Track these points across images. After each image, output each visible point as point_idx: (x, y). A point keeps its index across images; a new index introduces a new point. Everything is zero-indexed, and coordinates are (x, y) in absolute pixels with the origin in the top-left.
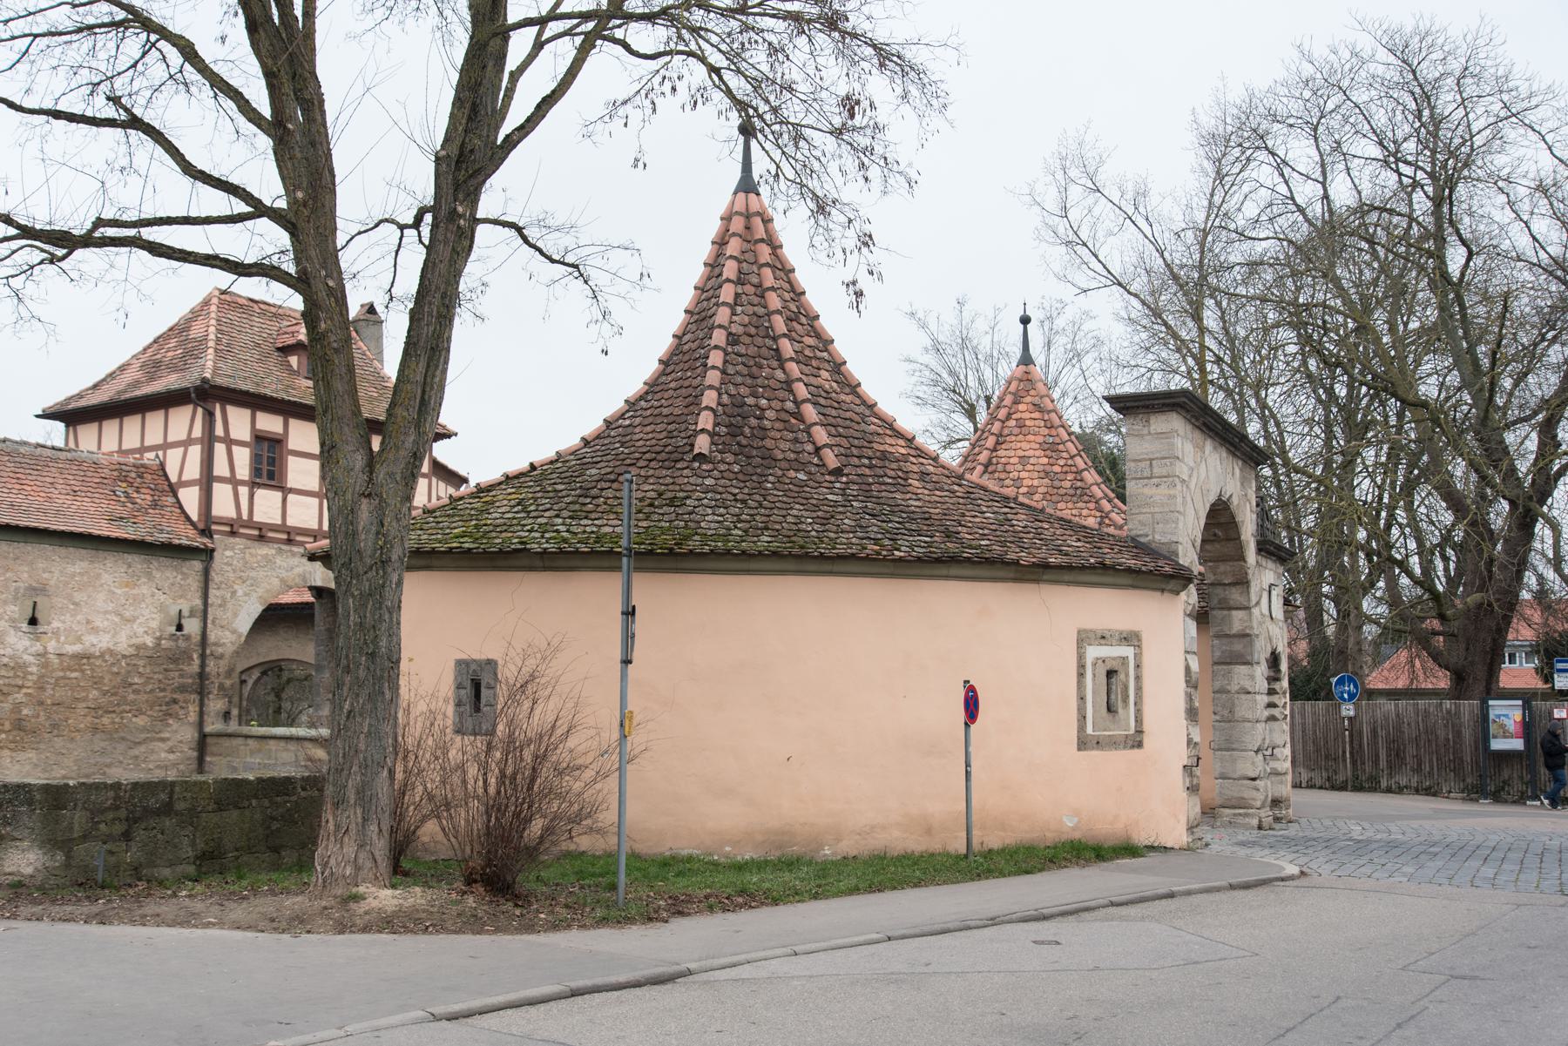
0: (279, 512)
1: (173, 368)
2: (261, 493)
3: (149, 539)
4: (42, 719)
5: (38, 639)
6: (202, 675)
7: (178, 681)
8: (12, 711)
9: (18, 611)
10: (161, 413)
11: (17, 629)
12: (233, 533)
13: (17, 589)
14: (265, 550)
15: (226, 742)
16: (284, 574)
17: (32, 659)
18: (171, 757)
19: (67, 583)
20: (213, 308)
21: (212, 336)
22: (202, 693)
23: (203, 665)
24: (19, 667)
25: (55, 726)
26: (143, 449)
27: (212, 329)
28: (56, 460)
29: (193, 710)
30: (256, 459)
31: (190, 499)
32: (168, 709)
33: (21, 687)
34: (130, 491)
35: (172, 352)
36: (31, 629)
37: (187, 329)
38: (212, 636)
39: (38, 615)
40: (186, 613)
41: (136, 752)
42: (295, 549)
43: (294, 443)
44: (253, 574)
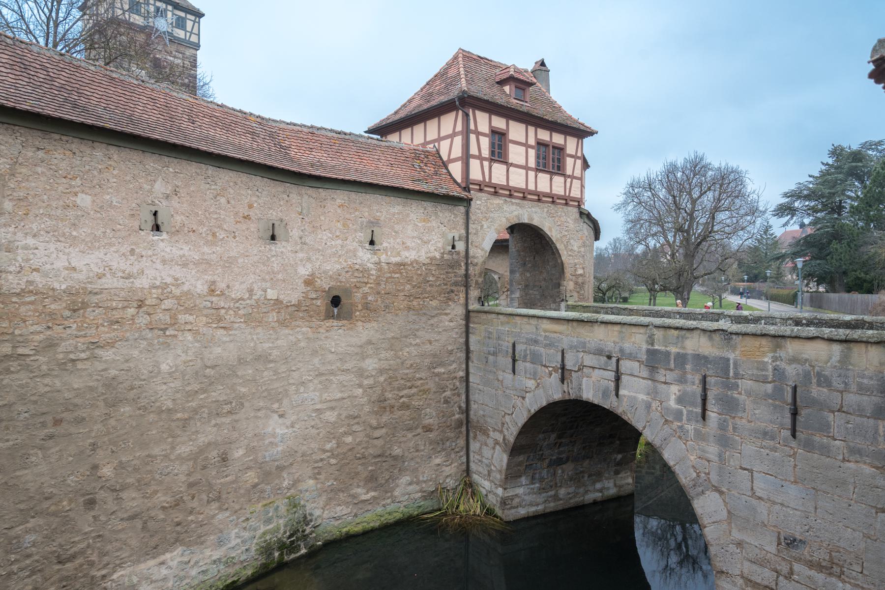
0: (505, 177)
1: (441, 94)
2: (496, 166)
3: (436, 192)
4: (379, 302)
6: (467, 276)
7: (454, 279)
9: (365, 236)
12: (481, 190)
13: (362, 222)
14: (497, 201)
15: (484, 316)
16: (508, 215)
17: (372, 266)
18: (451, 324)
19: (390, 219)
20: (460, 59)
21: (462, 72)
22: (467, 286)
23: (467, 270)
24: (365, 271)
25: (386, 307)
26: (426, 143)
27: (461, 69)
28: (380, 146)
29: (462, 296)
30: (492, 145)
31: (456, 170)
32: (449, 296)
34: (422, 165)
35: (439, 86)
36: (371, 247)
37: (447, 73)
38: (471, 253)
39: (375, 239)
40: (457, 238)
41: (432, 322)
42: (513, 201)
43: (512, 136)
44: (492, 215)
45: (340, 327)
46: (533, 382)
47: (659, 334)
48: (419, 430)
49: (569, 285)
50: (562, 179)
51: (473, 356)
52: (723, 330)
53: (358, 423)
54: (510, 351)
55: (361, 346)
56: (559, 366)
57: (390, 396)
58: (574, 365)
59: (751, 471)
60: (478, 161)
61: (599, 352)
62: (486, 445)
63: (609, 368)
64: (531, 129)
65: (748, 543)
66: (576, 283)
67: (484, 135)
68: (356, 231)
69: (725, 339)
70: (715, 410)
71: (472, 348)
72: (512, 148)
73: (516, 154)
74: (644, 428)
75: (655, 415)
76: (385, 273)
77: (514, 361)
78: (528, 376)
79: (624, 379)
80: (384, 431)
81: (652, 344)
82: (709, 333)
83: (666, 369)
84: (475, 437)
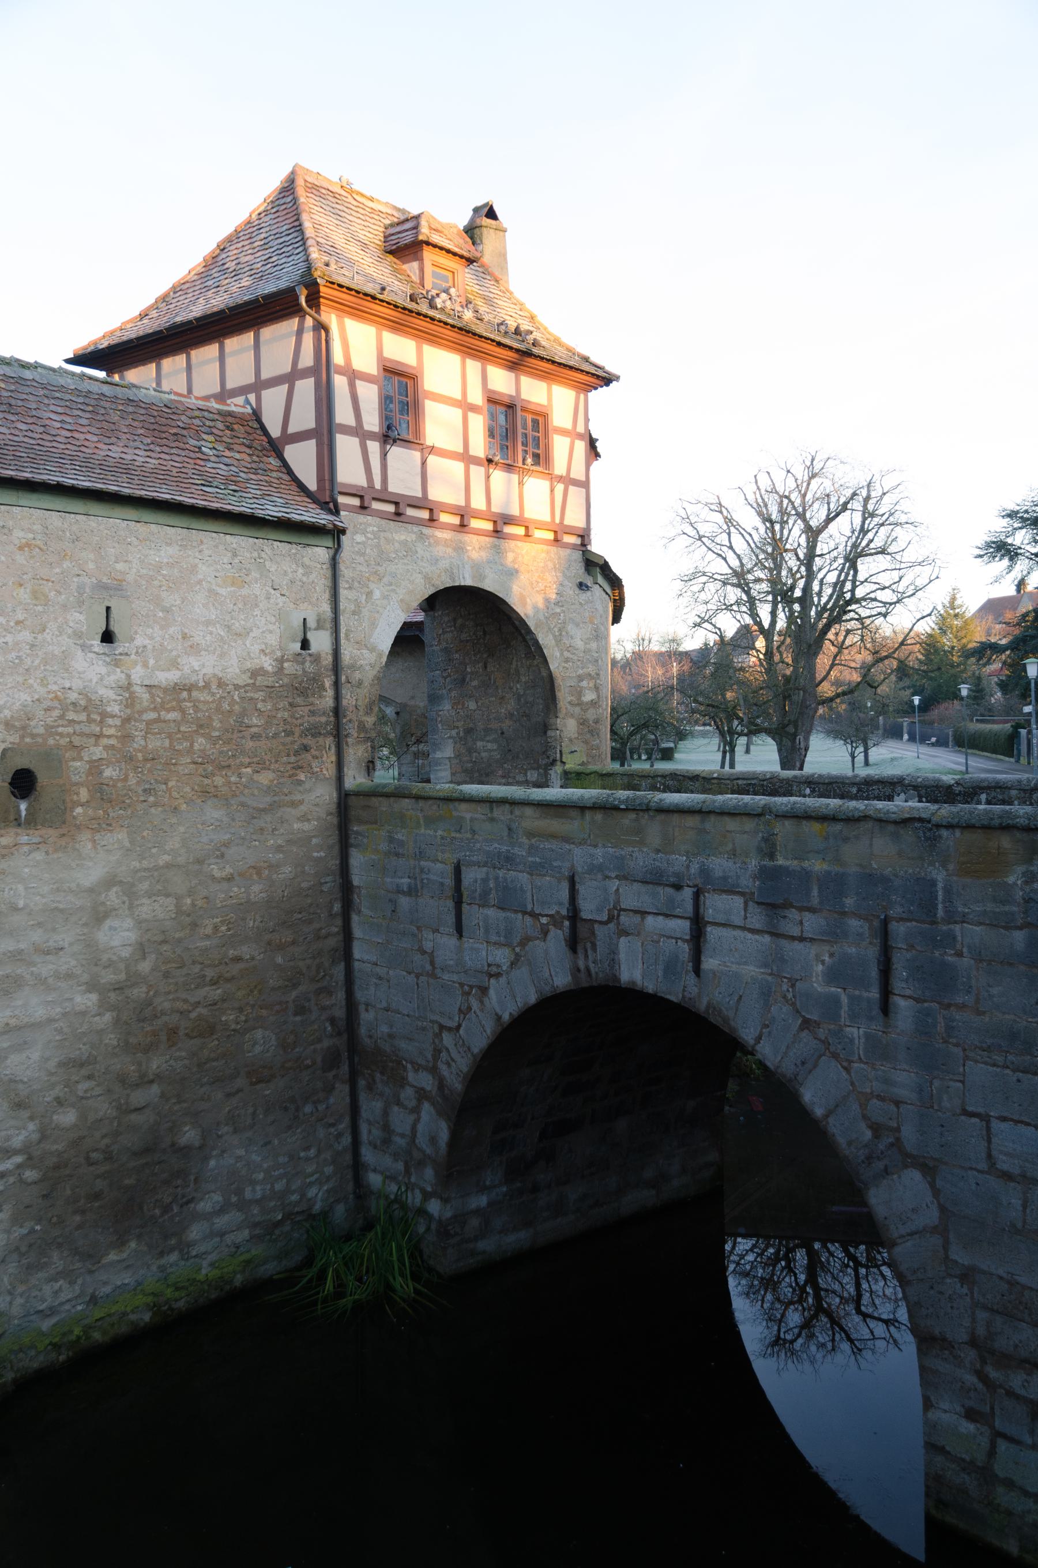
2: (396, 452)
4: (132, 781)
5: (117, 664)
6: (337, 711)
8: (90, 773)
10: (249, 337)
11: (85, 648)
13: (81, 588)
14: (402, 534)
17: (111, 694)
23: (337, 697)
24: (92, 707)
26: (223, 395)
30: (386, 400)
31: (303, 458)
33: (98, 737)
36: (105, 648)
39: (115, 627)
40: (312, 623)
43: (430, 382)
45: (36, 846)
46: (507, 951)
47: (783, 829)
48: (241, 1082)
49: (567, 726)
50: (544, 485)
51: (362, 902)
52: (920, 820)
53: (90, 1077)
54: (449, 882)
55: (91, 890)
56: (564, 912)
57: (167, 1005)
58: (599, 910)
59: (986, 1118)
60: (355, 441)
61: (654, 879)
62: (399, 1103)
63: (678, 911)
64: (473, 366)
65: (984, 1272)
66: (583, 722)
67: (367, 378)
68: (64, 607)
69: (927, 839)
70: (908, 992)
71: (356, 881)
72: (430, 407)
73: (440, 424)
74: (759, 1039)
75: (780, 1011)
76: (141, 713)
77: (458, 903)
78: (494, 938)
79: (712, 933)
80: (155, 1089)
81: (772, 856)
82: (891, 828)
83: (801, 909)
84: (370, 1088)
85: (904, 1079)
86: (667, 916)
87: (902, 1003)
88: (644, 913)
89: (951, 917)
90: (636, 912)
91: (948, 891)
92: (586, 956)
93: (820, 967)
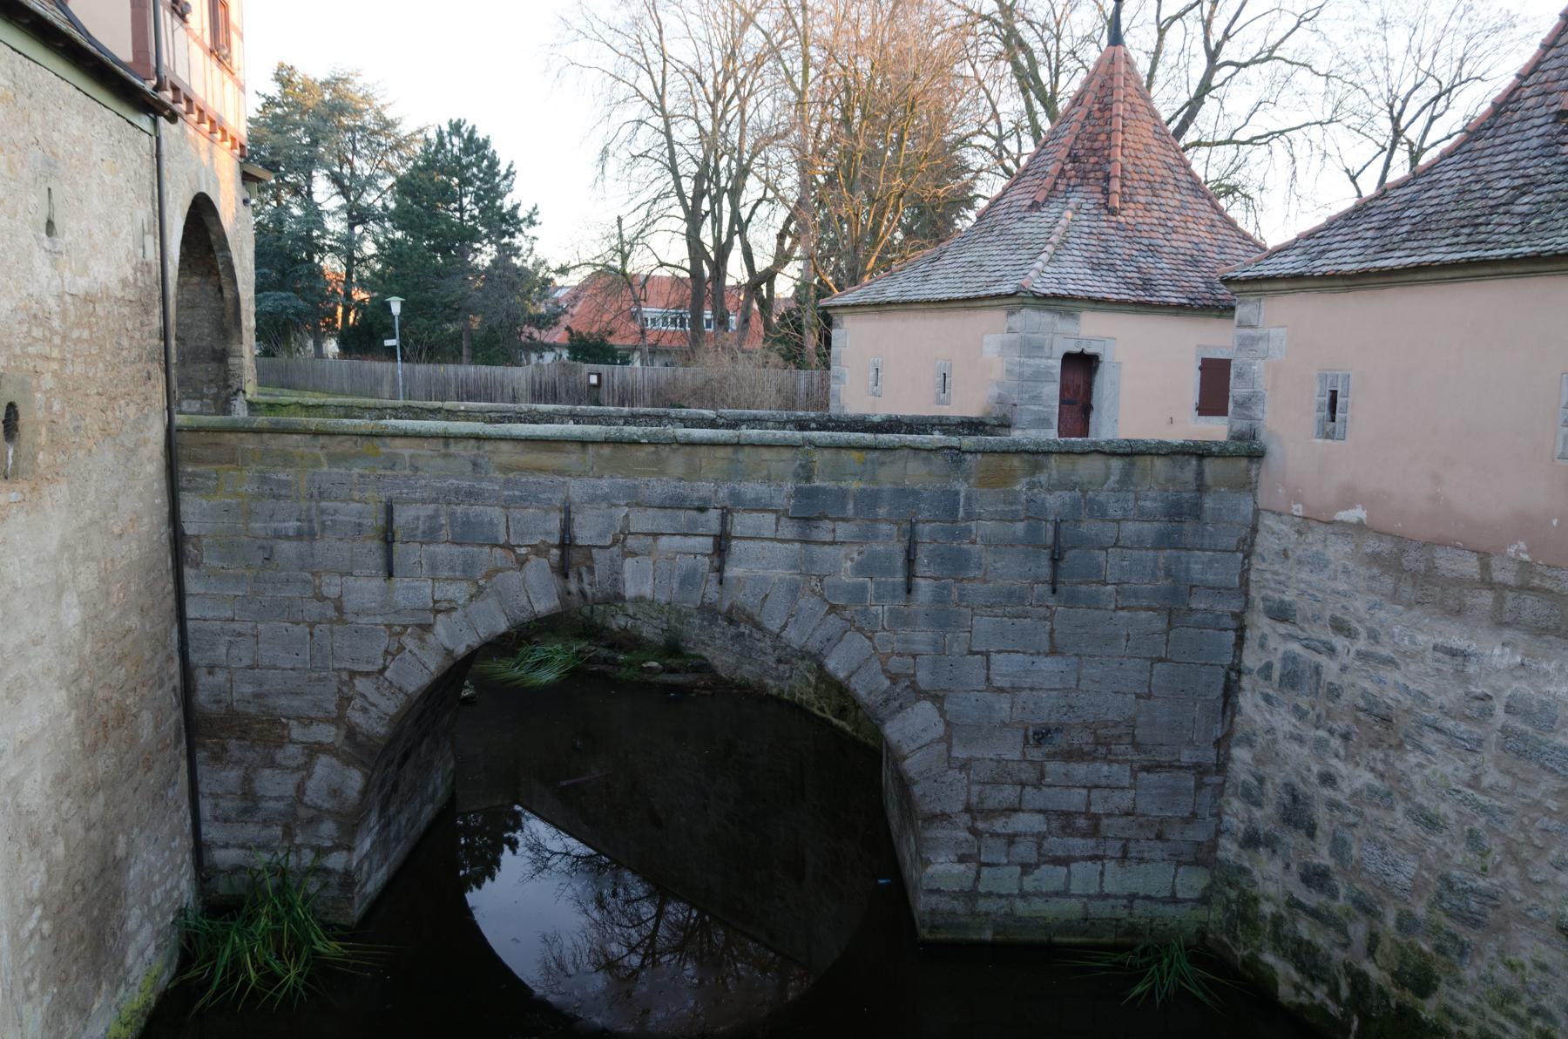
58: (601, 535)
59: (987, 654)
61: (676, 503)
75: (808, 603)
81: (808, 479)
82: (924, 454)
83: (834, 520)
85: (922, 638)
86: (686, 535)
87: (921, 582)
88: (656, 535)
89: (969, 516)
90: (646, 534)
91: (968, 498)
92: (580, 579)
93: (849, 564)
